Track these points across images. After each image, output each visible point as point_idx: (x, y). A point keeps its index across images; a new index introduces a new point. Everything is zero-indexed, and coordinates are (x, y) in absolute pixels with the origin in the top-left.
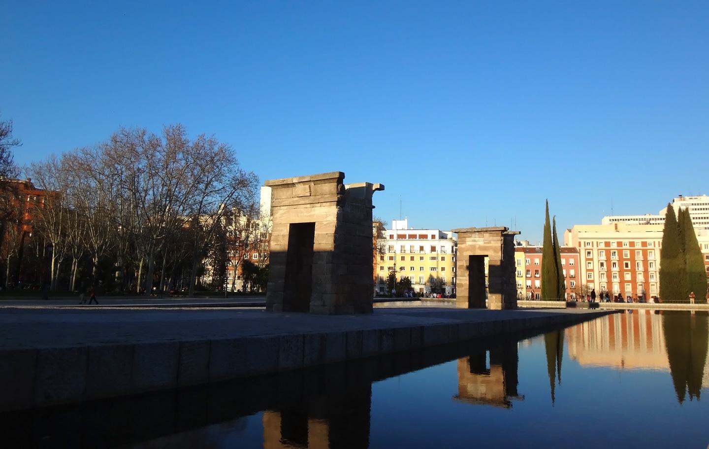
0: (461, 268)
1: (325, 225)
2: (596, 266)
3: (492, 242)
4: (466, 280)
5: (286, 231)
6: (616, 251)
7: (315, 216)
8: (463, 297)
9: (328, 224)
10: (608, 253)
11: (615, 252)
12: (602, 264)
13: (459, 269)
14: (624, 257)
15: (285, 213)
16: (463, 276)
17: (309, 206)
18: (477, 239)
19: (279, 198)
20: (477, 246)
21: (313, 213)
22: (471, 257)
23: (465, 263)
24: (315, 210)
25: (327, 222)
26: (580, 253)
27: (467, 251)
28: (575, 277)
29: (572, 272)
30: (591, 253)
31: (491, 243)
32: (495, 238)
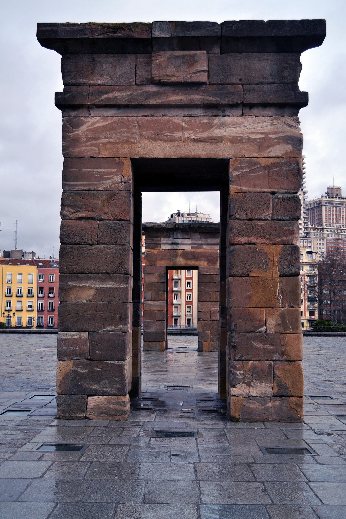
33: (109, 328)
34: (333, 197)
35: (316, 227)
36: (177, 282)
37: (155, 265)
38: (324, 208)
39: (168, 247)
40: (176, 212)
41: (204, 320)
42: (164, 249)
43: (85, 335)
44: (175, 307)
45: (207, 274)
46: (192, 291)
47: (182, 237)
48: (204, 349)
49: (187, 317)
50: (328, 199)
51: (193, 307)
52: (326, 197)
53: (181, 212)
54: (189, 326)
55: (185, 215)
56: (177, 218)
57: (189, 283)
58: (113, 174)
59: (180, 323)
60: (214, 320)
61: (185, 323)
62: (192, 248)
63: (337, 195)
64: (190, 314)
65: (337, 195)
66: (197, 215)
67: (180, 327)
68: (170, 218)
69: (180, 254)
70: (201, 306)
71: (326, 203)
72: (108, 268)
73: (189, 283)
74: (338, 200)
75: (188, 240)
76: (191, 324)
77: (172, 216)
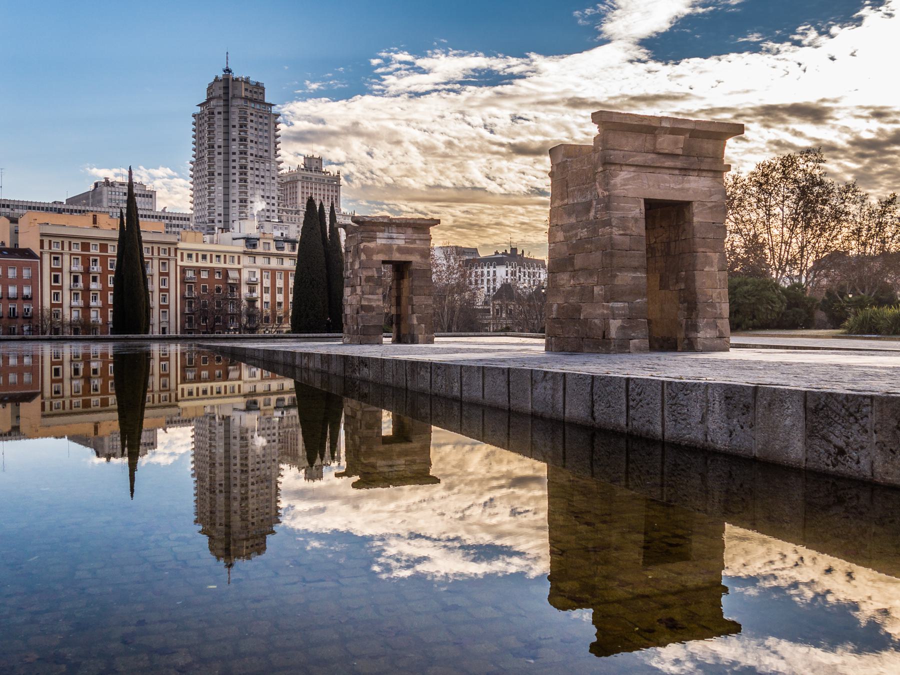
0: (369, 281)
1: (710, 208)
2: (67, 281)
3: (418, 242)
4: (379, 300)
5: (638, 211)
6: (98, 258)
7: (691, 192)
8: (374, 326)
9: (715, 207)
10: (86, 260)
11: (95, 261)
12: (76, 279)
14: (109, 269)
15: (633, 178)
16: (372, 294)
17: (677, 172)
18: (395, 235)
19: (617, 148)
20: (395, 247)
21: (687, 186)
23: (375, 273)
24: (689, 182)
25: (713, 204)
26: (41, 259)
27: (378, 253)
28: (31, 299)
29: (27, 291)
30: (60, 259)
31: (415, 243)
32: (422, 235)
33: (638, 300)
34: (311, 171)
35: (290, 208)
38: (300, 184)
39: (384, 241)
40: (104, 181)
43: (626, 304)
49: (161, 326)
50: (305, 172)
52: (302, 169)
53: (110, 181)
58: (636, 207)
63: (317, 168)
65: (317, 168)
68: (93, 187)
71: (303, 177)
72: (636, 264)
74: (318, 174)
77: (96, 185)
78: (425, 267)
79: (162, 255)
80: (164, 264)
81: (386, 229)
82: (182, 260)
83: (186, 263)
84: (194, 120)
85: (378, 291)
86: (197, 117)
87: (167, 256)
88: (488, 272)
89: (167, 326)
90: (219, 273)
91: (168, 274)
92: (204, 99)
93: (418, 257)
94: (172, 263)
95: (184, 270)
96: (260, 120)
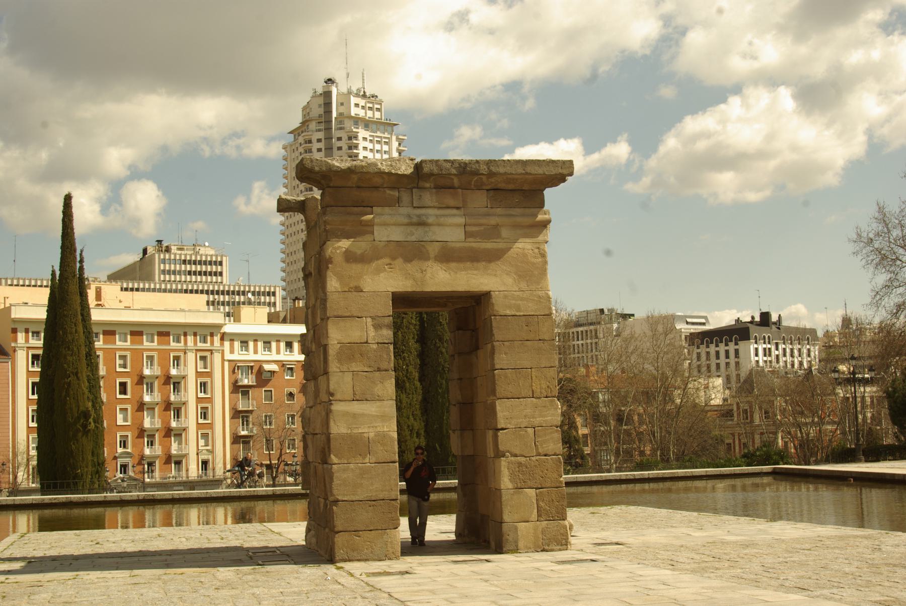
0: (351, 358)
4: (383, 418)
13: (340, 361)
14: (118, 369)
18: (431, 214)
20: (433, 249)
22: (401, 300)
31: (499, 236)
36: (179, 383)
37: (358, 290)
39: (397, 234)
41: (516, 456)
42: (385, 239)
44: (175, 435)
45: (518, 314)
46: (210, 400)
47: (436, 204)
48: (521, 544)
49: (202, 457)
51: (213, 434)
53: (165, 244)
54: (206, 474)
55: (174, 249)
56: (157, 256)
57: (204, 385)
59: (187, 470)
60: (545, 455)
61: (198, 470)
62: (468, 235)
64: (207, 450)
66: (198, 248)
67: (188, 477)
69: (432, 255)
70: (506, 413)
73: (204, 385)
75: (455, 211)
76: (210, 472)
77: (145, 251)
78: (530, 308)
79: (201, 345)
80: (203, 358)
81: (405, 197)
82: (232, 352)
83: (239, 355)
84: (285, 153)
85: (378, 390)
86: (288, 149)
87: (207, 346)
88: (727, 352)
89: (210, 457)
90: (291, 369)
91: (210, 375)
92: (296, 121)
93: (509, 281)
94: (217, 357)
95: (235, 367)
96: (378, 147)
